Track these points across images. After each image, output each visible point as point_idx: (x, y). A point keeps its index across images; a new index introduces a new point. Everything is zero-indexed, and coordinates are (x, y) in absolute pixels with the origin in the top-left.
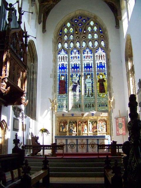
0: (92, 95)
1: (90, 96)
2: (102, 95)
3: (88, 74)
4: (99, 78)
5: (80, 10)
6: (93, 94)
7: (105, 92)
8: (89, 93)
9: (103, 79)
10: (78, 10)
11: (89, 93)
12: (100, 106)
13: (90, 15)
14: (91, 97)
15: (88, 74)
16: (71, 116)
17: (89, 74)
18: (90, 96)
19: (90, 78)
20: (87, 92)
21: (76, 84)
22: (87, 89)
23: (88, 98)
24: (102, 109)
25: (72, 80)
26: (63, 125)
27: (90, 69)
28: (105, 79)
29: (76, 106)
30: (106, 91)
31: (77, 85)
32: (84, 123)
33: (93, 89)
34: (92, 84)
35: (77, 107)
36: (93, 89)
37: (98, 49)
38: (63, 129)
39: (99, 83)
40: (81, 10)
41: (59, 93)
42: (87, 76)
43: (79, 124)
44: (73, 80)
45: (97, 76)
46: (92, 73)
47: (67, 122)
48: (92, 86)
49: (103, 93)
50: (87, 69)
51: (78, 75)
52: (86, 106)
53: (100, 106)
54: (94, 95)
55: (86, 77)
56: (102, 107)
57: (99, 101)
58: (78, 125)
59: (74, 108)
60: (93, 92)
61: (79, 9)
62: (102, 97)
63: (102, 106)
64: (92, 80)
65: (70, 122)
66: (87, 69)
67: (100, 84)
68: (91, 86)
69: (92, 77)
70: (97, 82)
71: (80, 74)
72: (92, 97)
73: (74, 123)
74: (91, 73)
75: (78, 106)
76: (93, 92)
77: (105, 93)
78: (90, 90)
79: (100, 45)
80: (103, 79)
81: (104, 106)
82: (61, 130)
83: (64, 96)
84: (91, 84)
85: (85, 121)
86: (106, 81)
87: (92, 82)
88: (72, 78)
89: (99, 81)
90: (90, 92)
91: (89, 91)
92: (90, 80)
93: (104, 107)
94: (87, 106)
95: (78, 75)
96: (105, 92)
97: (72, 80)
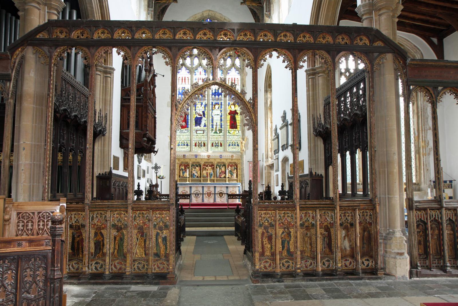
0: (221, 131)
1: (218, 132)
2: (233, 131)
3: (216, 104)
4: (230, 109)
5: (209, 10)
6: (222, 130)
7: (236, 128)
9: (236, 111)
10: (207, 11)
12: (229, 145)
13: (223, 19)
14: (220, 133)
15: (216, 104)
16: (194, 157)
17: (218, 104)
18: (218, 132)
19: (218, 108)
20: (214, 127)
21: (199, 116)
22: (215, 124)
23: (216, 134)
24: (233, 150)
25: (195, 110)
26: (183, 168)
27: (218, 96)
28: (237, 111)
29: (200, 144)
30: (238, 127)
31: (202, 117)
32: (210, 166)
33: (221, 124)
34: (221, 116)
35: (201, 146)
36: (221, 124)
37: (230, 69)
38: (183, 173)
39: (229, 116)
40: (211, 11)
42: (215, 106)
43: (203, 168)
44: (196, 111)
45: (228, 106)
46: (221, 103)
47: (189, 165)
48: (221, 120)
49: (234, 129)
50: (215, 96)
51: (204, 104)
52: (212, 144)
53: (229, 145)
54: (223, 131)
55: (213, 106)
56: (232, 147)
57: (229, 140)
58: (203, 169)
59: (197, 147)
60: (221, 127)
61: (209, 9)
62: (233, 134)
63: (232, 145)
64: (221, 111)
65: (192, 165)
66: (215, 96)
67: (231, 117)
68: (219, 119)
69: (221, 108)
70: (228, 114)
71: (206, 103)
72: (221, 134)
73: (198, 167)
74: (220, 102)
75: (203, 145)
76: (221, 127)
77: (236, 129)
78: (218, 124)
79: (233, 65)
80: (236, 111)
81: (235, 145)
82: (181, 175)
83: (184, 131)
84: (219, 116)
85: (210, 164)
86: (239, 114)
87: (222, 114)
88: (195, 107)
89: (229, 114)
90: (218, 126)
91: (217, 125)
92: (219, 112)
93: (235, 147)
94: (214, 145)
95: (204, 104)
96: (236, 128)
97: (195, 110)
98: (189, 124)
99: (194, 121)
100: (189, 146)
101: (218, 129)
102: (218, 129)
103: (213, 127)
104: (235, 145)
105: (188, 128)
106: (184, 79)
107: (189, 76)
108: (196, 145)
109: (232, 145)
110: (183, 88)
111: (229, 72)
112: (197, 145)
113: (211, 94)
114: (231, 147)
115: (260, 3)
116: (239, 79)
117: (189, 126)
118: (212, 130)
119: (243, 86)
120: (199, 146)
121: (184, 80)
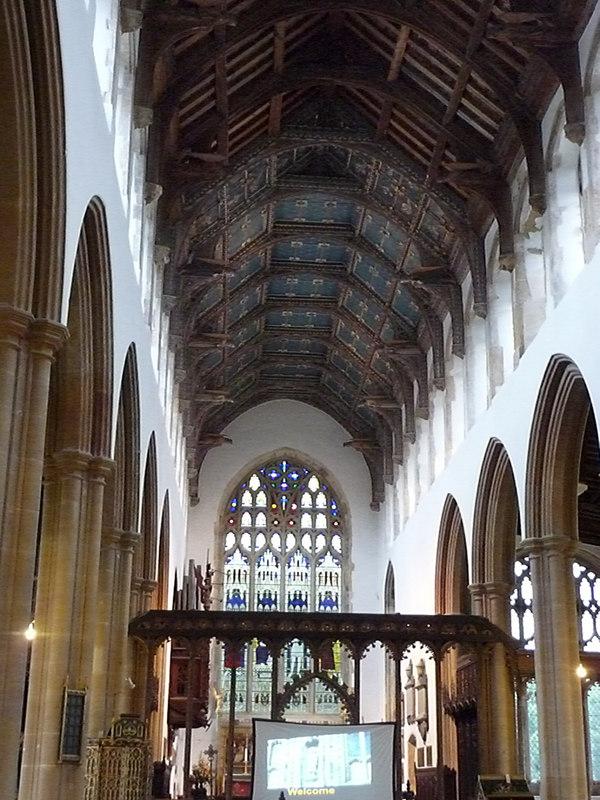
8: (296, 668)
11: (296, 668)
12: (320, 702)
20: (293, 665)
22: (293, 660)
30: (336, 665)
37: (323, 555)
41: (225, 666)
47: (244, 740)
53: (320, 702)
78: (299, 661)
79: (329, 548)
91: (296, 662)
98: (246, 659)
99: (255, 654)
100: (244, 703)
101: (299, 670)
102: (299, 670)
103: (289, 666)
104: (330, 702)
105: (243, 666)
106: (237, 573)
107: (247, 568)
108: (257, 701)
109: (326, 701)
110: (235, 590)
111: (321, 561)
112: (260, 700)
113: (287, 602)
114: (323, 704)
115: (377, 445)
116: (340, 575)
117: (246, 663)
118: (289, 671)
119: (347, 589)
120: (262, 702)
121: (237, 576)
